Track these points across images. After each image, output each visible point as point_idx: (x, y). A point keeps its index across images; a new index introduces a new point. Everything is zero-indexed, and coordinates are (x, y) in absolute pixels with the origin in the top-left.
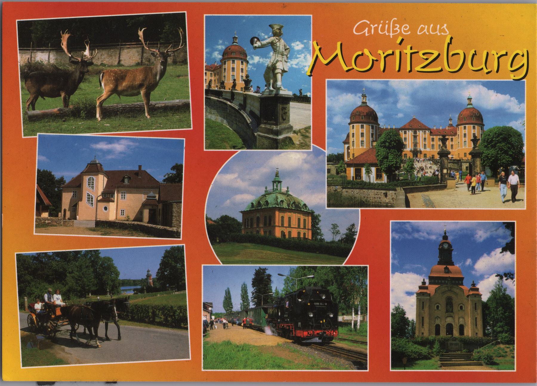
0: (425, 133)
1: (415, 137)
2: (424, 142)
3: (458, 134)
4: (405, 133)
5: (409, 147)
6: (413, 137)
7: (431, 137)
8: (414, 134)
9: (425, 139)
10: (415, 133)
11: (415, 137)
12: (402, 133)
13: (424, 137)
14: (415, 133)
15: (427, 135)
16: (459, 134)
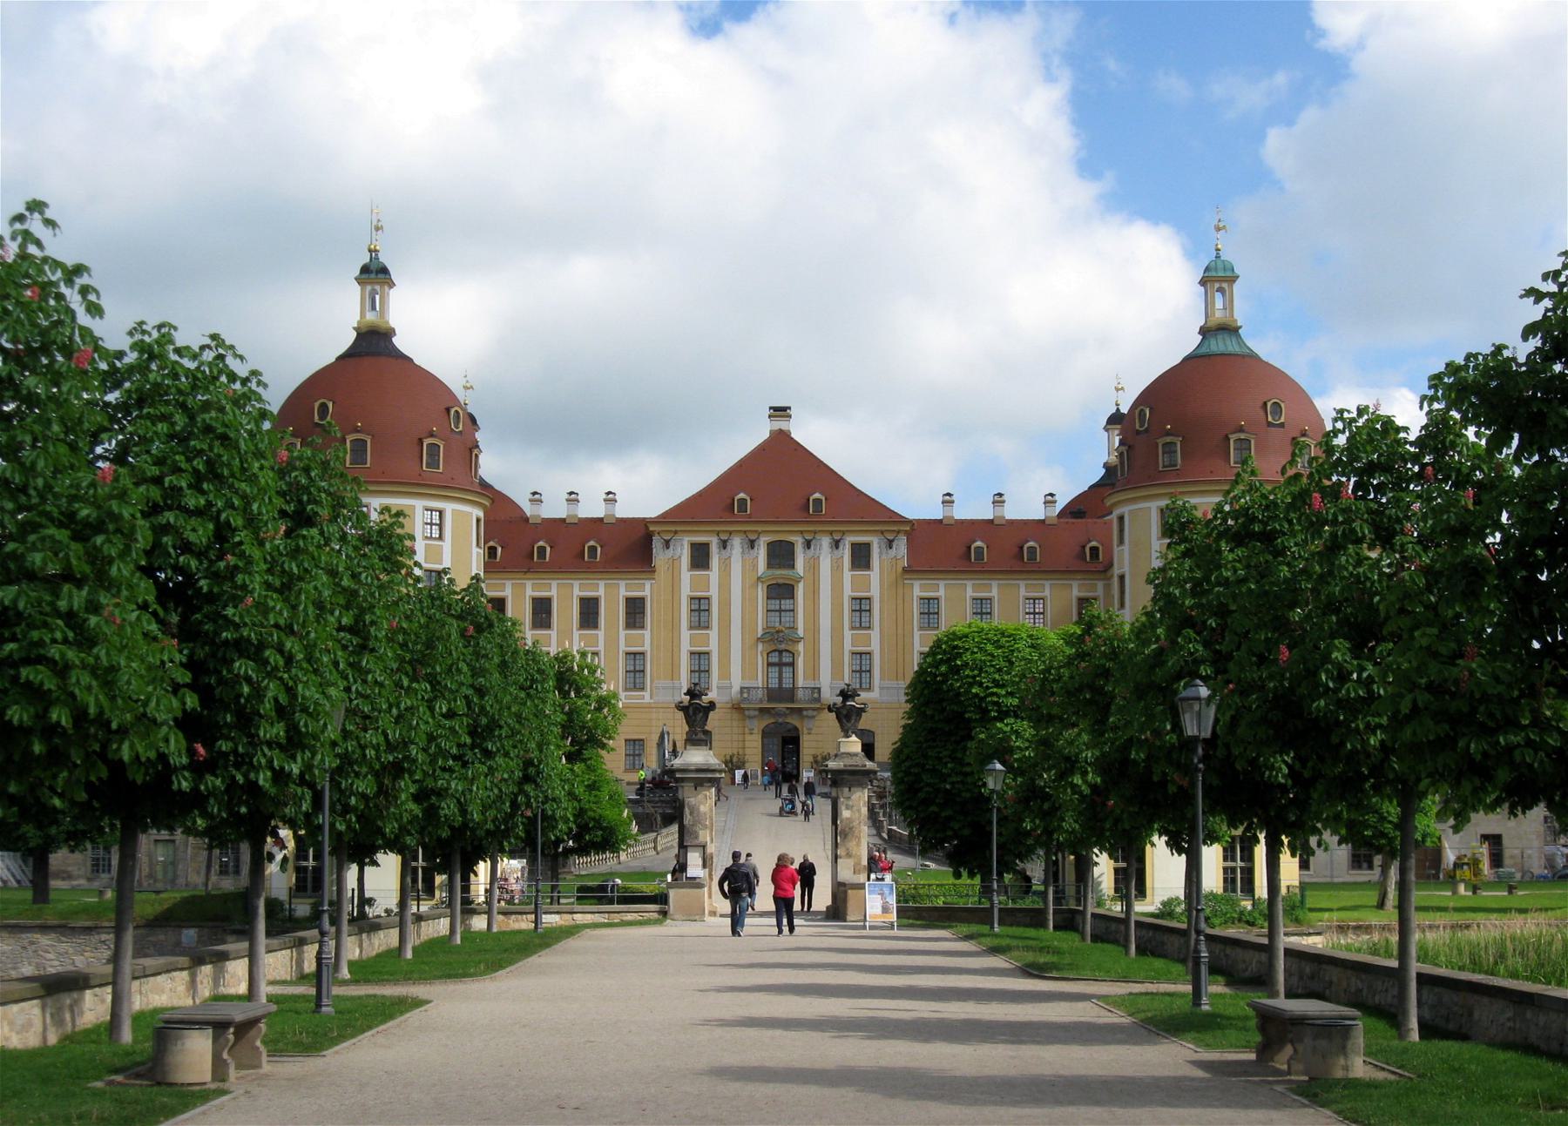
0: (861, 557)
1: (781, 592)
2: (848, 634)
3: (1116, 571)
4: (700, 557)
5: (725, 674)
6: (761, 592)
7: (918, 589)
8: (770, 565)
9: (861, 606)
10: (781, 555)
11: (781, 592)
12: (675, 561)
13: (848, 592)
14: (781, 555)
15: (875, 575)
16: (1126, 570)
